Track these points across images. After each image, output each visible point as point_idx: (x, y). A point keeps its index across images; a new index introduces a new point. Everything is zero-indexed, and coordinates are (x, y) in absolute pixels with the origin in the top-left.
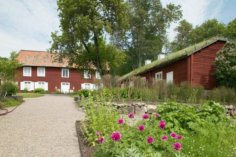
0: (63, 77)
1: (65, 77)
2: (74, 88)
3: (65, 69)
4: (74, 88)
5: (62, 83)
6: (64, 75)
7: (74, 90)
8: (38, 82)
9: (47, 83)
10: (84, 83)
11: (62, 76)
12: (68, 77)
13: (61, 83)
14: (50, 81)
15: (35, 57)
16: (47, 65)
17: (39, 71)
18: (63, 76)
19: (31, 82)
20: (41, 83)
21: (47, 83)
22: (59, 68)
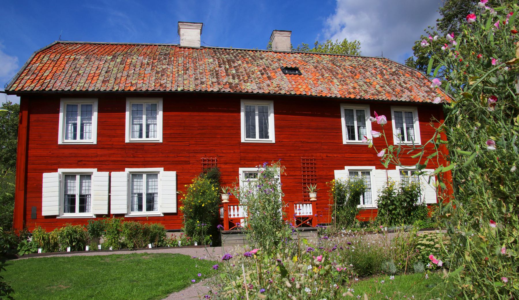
0: (251, 140)
1: (257, 139)
2: (313, 196)
3: (256, 105)
4: (313, 196)
5: (241, 170)
6: (250, 133)
7: (316, 205)
8: (128, 170)
9: (173, 174)
10: (347, 168)
11: (244, 139)
12: (272, 138)
13: (241, 170)
14: (187, 163)
15: (114, 57)
16: (170, 87)
17: (133, 113)
18: (248, 136)
19: (94, 171)
20: (145, 176)
21: (173, 174)
22: (229, 94)
